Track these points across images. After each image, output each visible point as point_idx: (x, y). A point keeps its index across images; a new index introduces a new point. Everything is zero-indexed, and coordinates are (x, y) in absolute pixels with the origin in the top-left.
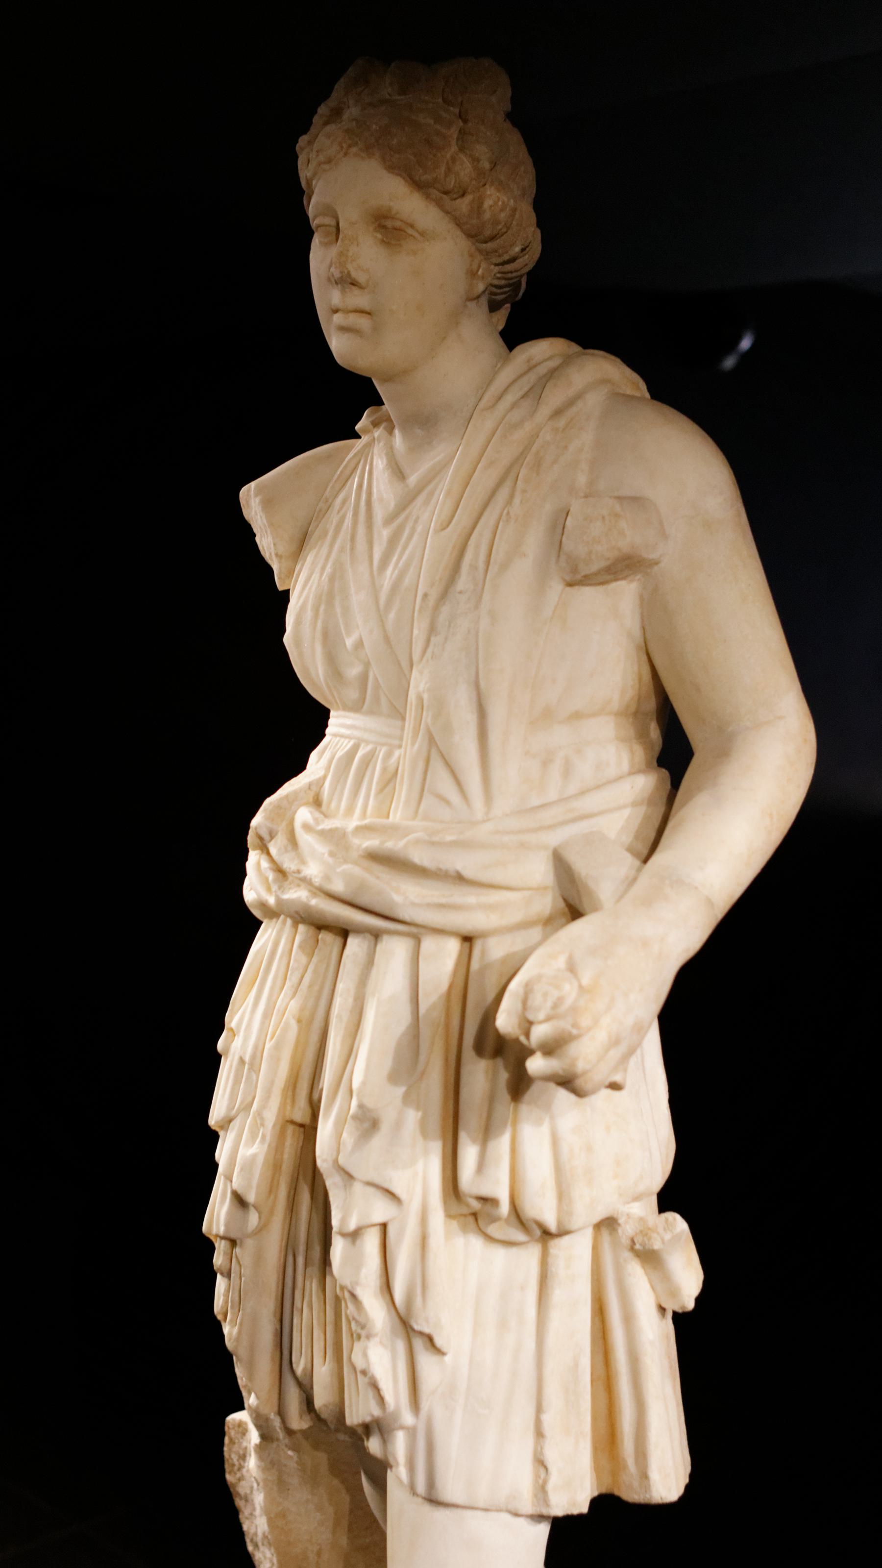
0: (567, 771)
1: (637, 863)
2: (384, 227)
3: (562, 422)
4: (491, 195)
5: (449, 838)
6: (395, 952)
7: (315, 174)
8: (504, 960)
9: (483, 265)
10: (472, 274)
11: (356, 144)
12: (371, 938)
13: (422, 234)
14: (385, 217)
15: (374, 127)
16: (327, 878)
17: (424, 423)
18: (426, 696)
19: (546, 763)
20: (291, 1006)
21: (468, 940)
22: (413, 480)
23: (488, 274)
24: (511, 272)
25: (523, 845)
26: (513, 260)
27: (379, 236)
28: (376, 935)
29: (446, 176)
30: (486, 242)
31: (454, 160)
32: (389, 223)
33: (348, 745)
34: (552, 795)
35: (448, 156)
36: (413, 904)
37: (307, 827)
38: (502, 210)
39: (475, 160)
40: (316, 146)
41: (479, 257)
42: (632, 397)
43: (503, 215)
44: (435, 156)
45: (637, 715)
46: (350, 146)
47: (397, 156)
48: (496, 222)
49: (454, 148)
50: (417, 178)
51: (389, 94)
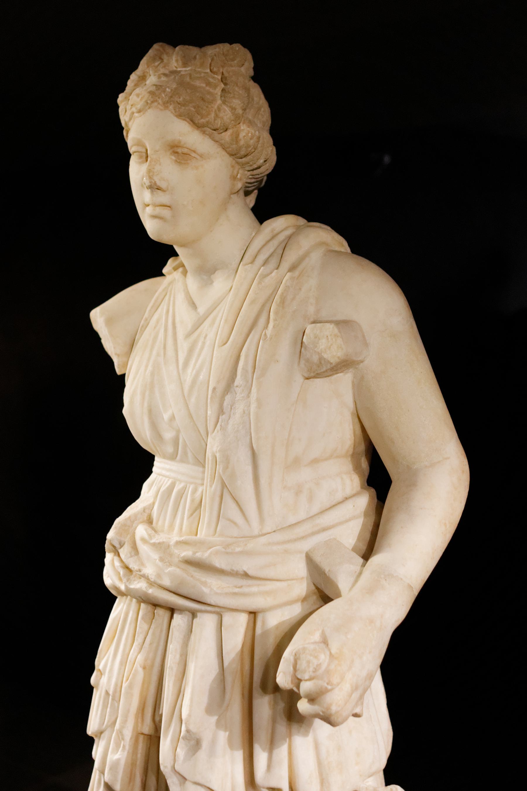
0: (311, 499)
1: (361, 560)
2: (177, 153)
3: (296, 273)
4: (243, 130)
5: (238, 549)
6: (206, 623)
7: (130, 119)
8: (277, 627)
9: (241, 171)
10: (234, 178)
11: (156, 101)
12: (190, 615)
13: (201, 156)
14: (177, 146)
15: (167, 89)
16: (159, 576)
17: (207, 272)
18: (218, 455)
19: (298, 493)
20: (139, 658)
21: (253, 614)
22: (202, 310)
23: (244, 177)
24: (258, 175)
25: (286, 551)
26: (259, 168)
27: (173, 158)
28: (194, 614)
29: (215, 120)
30: (241, 158)
31: (219, 109)
32: (179, 150)
33: (168, 483)
34: (302, 515)
35: (216, 107)
36: (216, 593)
37: (143, 540)
38: (251, 139)
39: (233, 109)
40: (130, 102)
41: (237, 167)
42: (340, 252)
43: (252, 141)
44: (207, 107)
45: (354, 456)
46: (152, 102)
47: (183, 108)
48: (248, 146)
49: (219, 102)
50: (197, 122)
51: (176, 67)
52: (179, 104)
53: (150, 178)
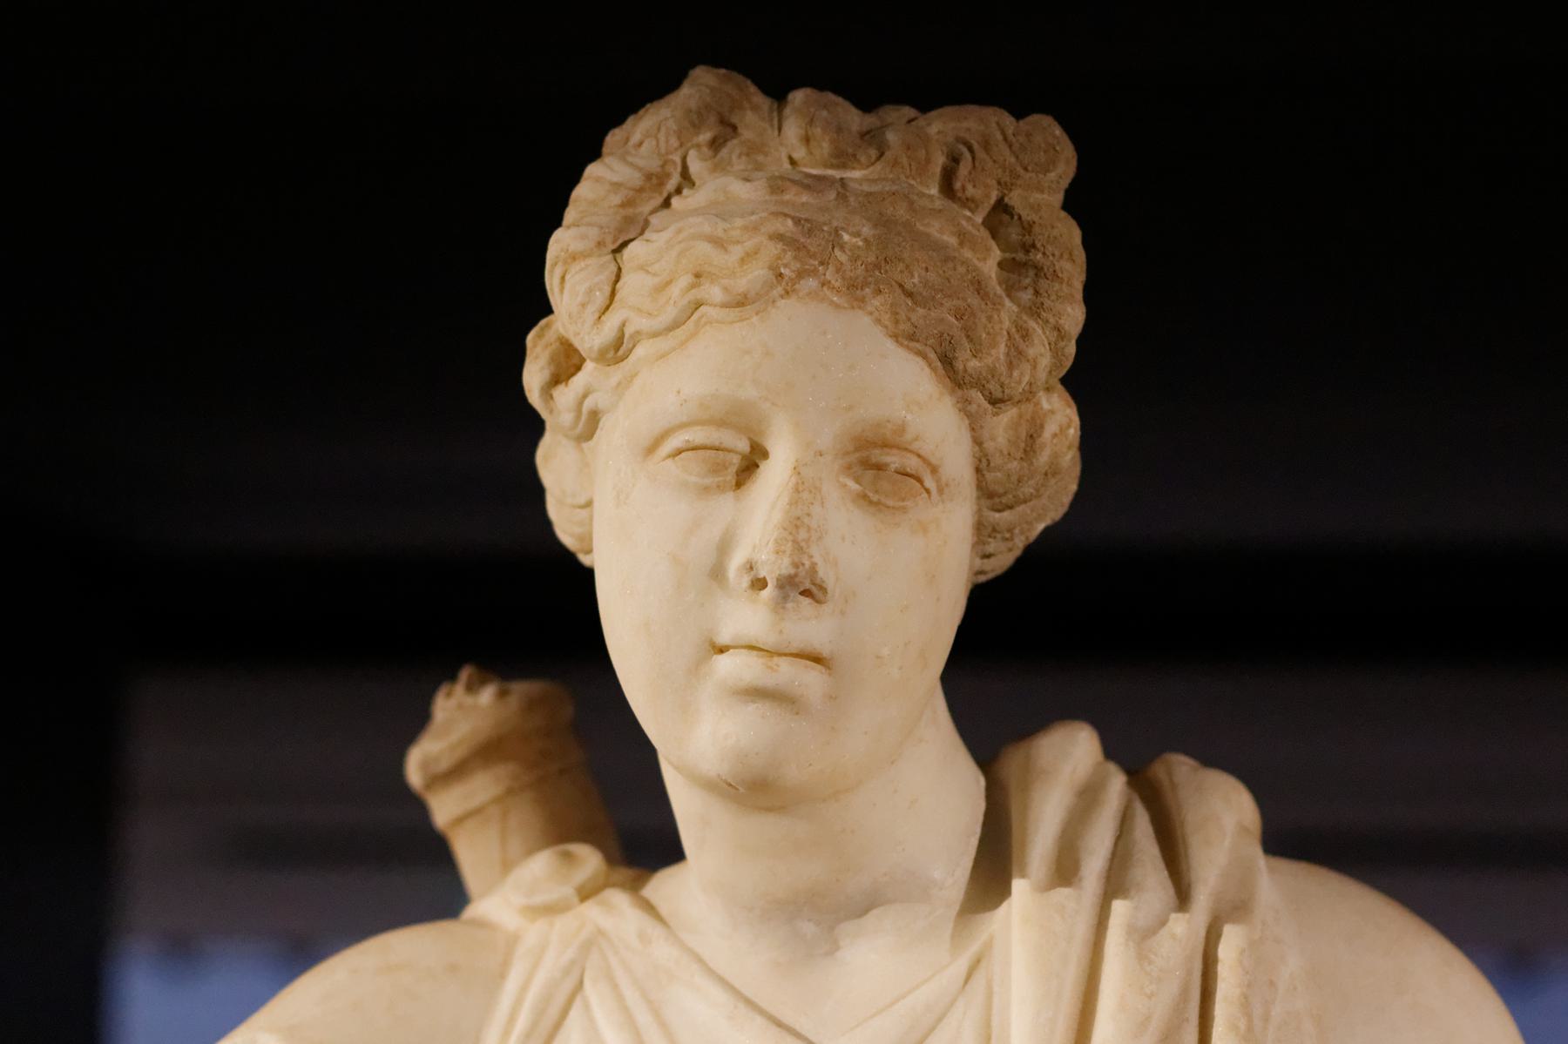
2: (879, 467)
4: (1052, 412)
11: (813, 273)
14: (886, 445)
29: (1011, 366)
32: (894, 460)
46: (801, 275)
47: (921, 311)
52: (910, 295)
53: (799, 548)
